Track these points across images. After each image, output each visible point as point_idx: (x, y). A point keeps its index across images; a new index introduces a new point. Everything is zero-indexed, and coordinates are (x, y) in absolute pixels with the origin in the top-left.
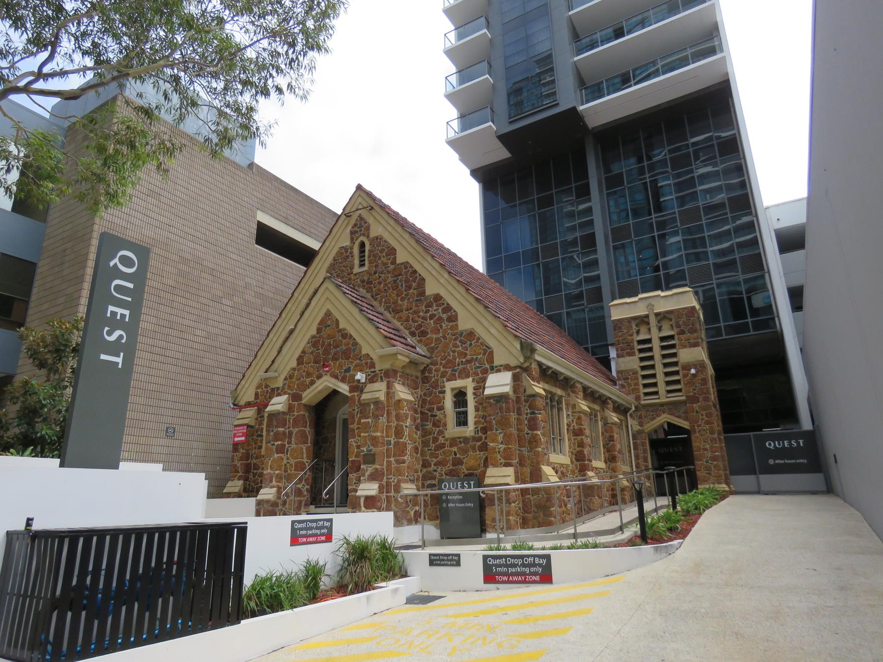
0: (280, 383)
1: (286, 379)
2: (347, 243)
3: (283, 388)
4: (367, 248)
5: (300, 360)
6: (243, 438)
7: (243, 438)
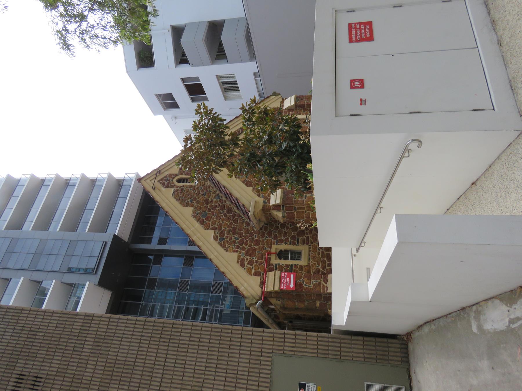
0: (261, 200)
1: (259, 196)
2: (172, 190)
3: (265, 198)
4: (184, 176)
5: (248, 184)
6: (292, 276)
7: (292, 276)
